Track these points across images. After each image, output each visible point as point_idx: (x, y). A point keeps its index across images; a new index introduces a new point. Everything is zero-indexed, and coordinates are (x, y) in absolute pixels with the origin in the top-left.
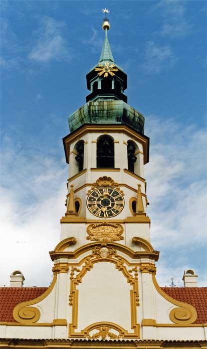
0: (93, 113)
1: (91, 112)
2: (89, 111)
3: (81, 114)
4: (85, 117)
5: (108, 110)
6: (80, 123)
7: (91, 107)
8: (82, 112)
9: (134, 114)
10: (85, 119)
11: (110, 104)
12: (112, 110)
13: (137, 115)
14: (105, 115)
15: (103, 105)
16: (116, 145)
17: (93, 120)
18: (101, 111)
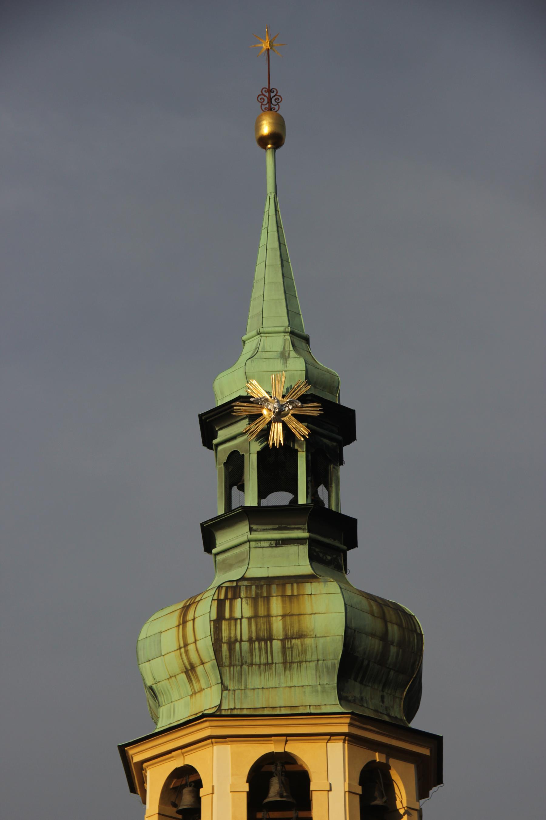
0: (231, 649)
1: (225, 648)
2: (217, 651)
3: (186, 645)
4: (203, 663)
5: (286, 638)
6: (184, 676)
7: (225, 624)
8: (190, 639)
9: (384, 637)
10: (200, 670)
11: (296, 612)
12: (301, 636)
13: (394, 631)
14: (278, 657)
15: (268, 616)
16: (317, 800)
17: (232, 678)
18: (259, 640)
